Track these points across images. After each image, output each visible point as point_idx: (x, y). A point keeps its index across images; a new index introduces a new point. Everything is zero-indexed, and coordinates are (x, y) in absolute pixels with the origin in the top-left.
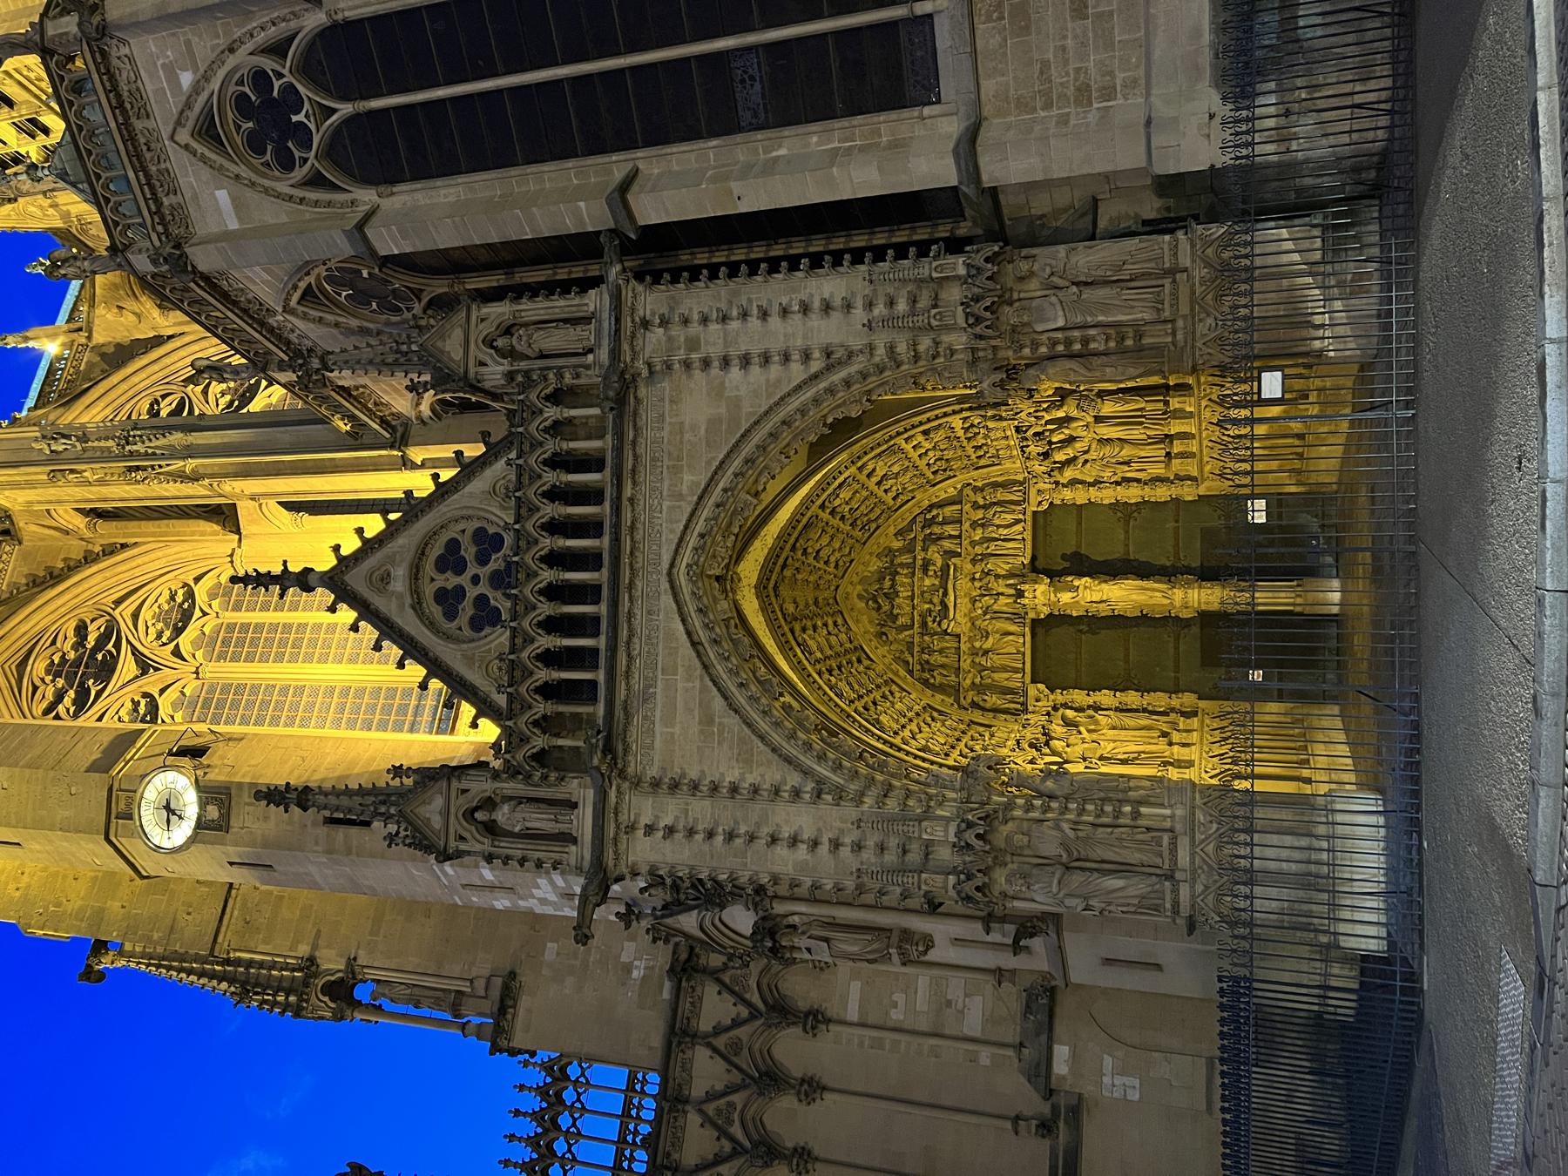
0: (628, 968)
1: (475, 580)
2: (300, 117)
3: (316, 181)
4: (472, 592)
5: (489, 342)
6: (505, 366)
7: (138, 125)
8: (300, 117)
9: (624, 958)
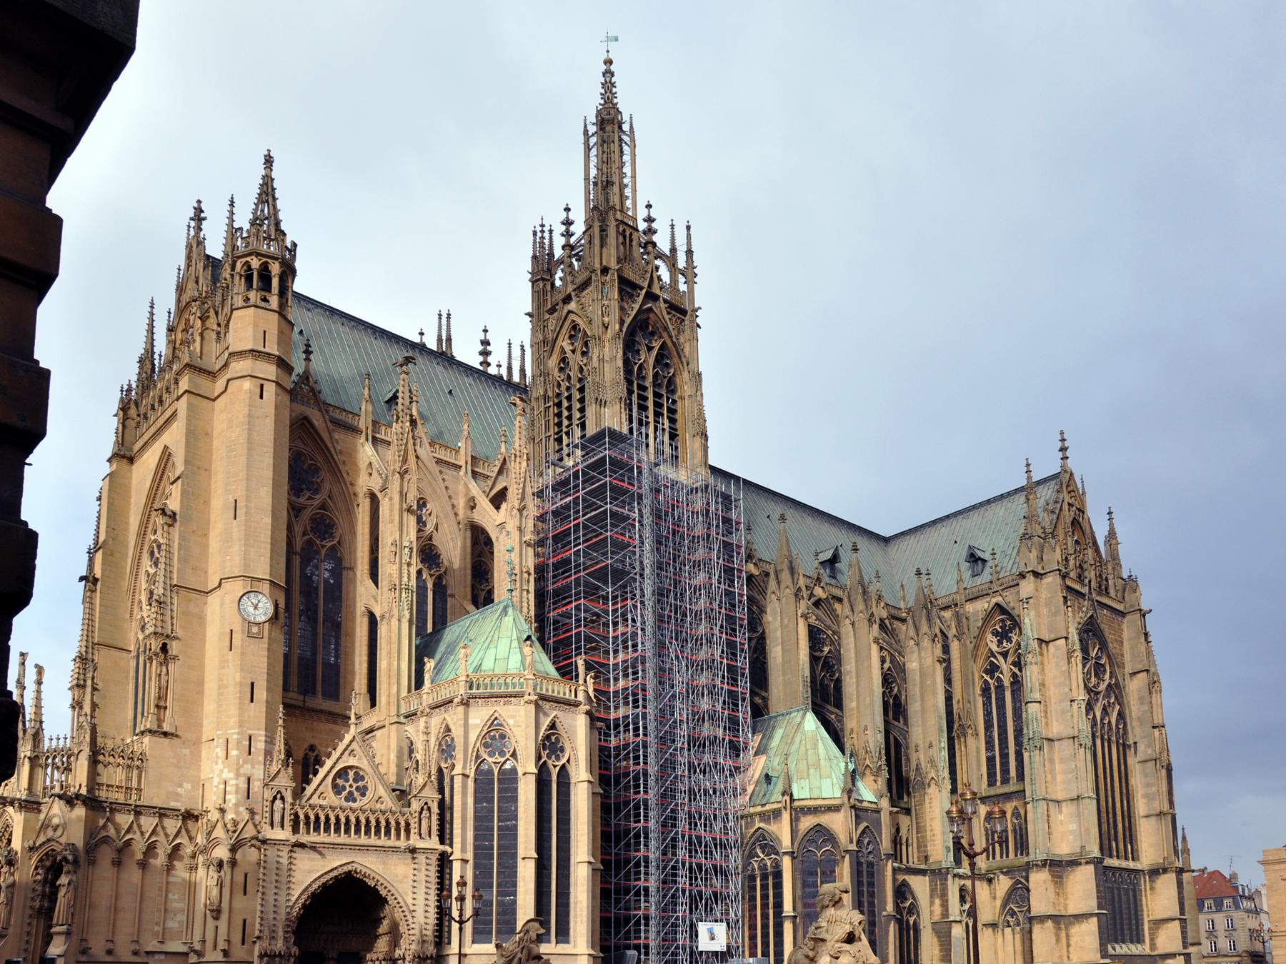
0: (180, 786)
1: (351, 786)
2: (497, 755)
3: (478, 757)
4: (348, 789)
5: (426, 803)
6: (419, 810)
7: (502, 700)
8: (497, 755)
9: (185, 784)
